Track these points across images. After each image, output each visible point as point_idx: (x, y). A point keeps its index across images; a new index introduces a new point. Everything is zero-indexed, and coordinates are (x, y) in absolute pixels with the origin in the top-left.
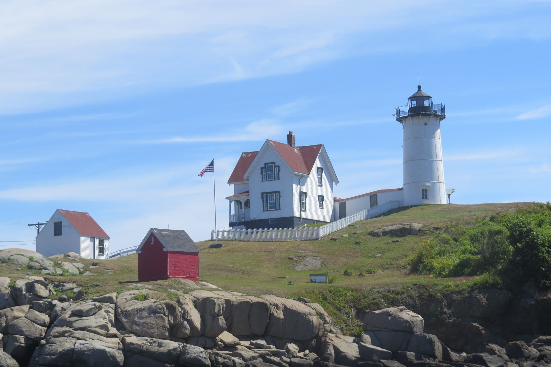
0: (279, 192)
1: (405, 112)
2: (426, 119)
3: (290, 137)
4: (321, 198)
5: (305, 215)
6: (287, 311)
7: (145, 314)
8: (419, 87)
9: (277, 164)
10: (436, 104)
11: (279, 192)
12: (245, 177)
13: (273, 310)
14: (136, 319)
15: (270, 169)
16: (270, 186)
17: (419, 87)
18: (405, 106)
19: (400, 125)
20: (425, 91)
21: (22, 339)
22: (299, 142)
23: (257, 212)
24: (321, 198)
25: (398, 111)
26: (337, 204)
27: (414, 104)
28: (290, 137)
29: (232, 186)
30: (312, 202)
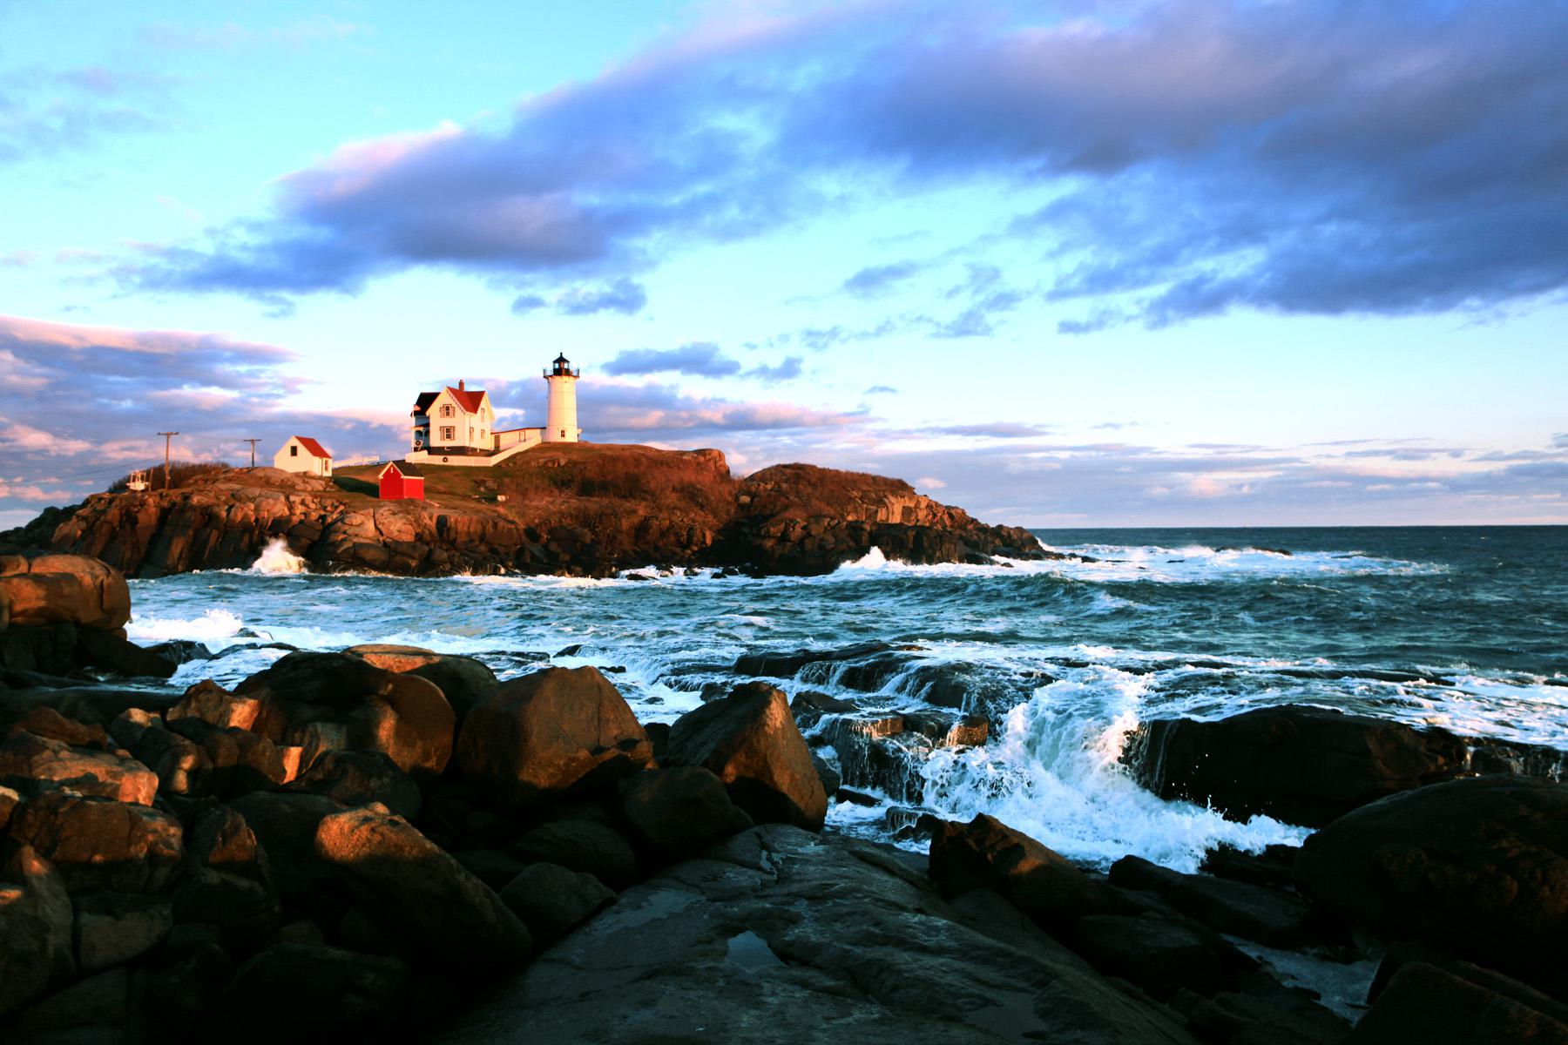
1: (550, 372)
3: (461, 384)
4: (483, 431)
5: (473, 445)
10: (572, 366)
16: (448, 422)
22: (468, 388)
23: (436, 440)
24: (483, 431)
28: (461, 384)
30: (477, 433)
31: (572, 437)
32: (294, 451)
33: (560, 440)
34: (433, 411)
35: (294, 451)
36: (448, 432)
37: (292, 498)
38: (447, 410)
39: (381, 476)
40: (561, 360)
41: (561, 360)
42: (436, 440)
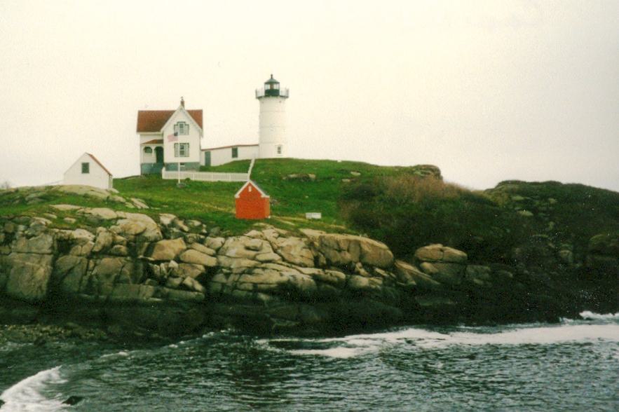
0: (188, 144)
2: (279, 99)
3: (182, 103)
6: (372, 245)
7: (298, 249)
8: (272, 76)
9: (187, 123)
10: (282, 88)
11: (188, 144)
12: (162, 130)
13: (363, 246)
14: (292, 252)
15: (181, 126)
16: (181, 139)
17: (272, 76)
18: (262, 88)
19: (258, 101)
20: (276, 78)
21: (202, 268)
22: (188, 107)
25: (256, 92)
26: (203, 153)
27: (268, 87)
28: (182, 103)
29: (139, 136)
31: (284, 155)
32: (85, 168)
33: (275, 155)
34: (168, 129)
35: (85, 168)
36: (183, 149)
37: (166, 219)
38: (181, 125)
39: (237, 196)
40: (271, 82)
41: (271, 82)
42: (169, 157)
